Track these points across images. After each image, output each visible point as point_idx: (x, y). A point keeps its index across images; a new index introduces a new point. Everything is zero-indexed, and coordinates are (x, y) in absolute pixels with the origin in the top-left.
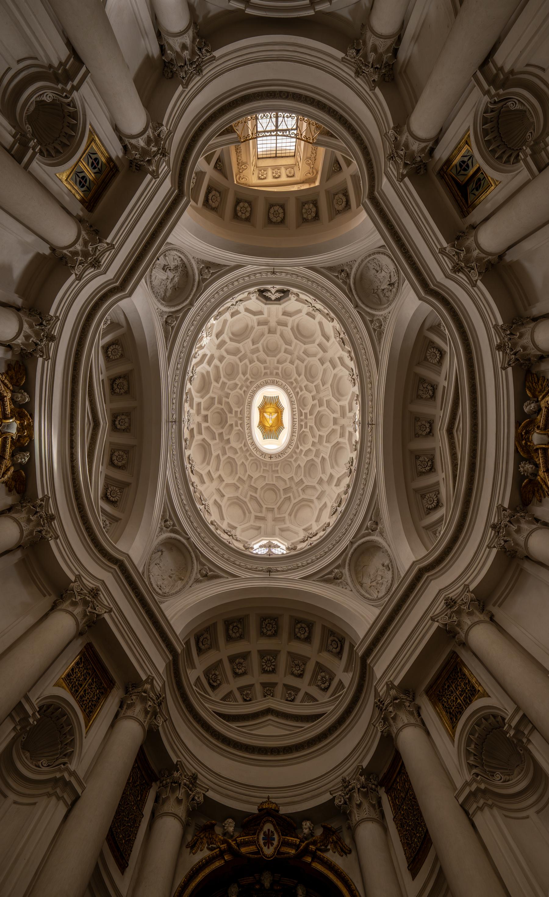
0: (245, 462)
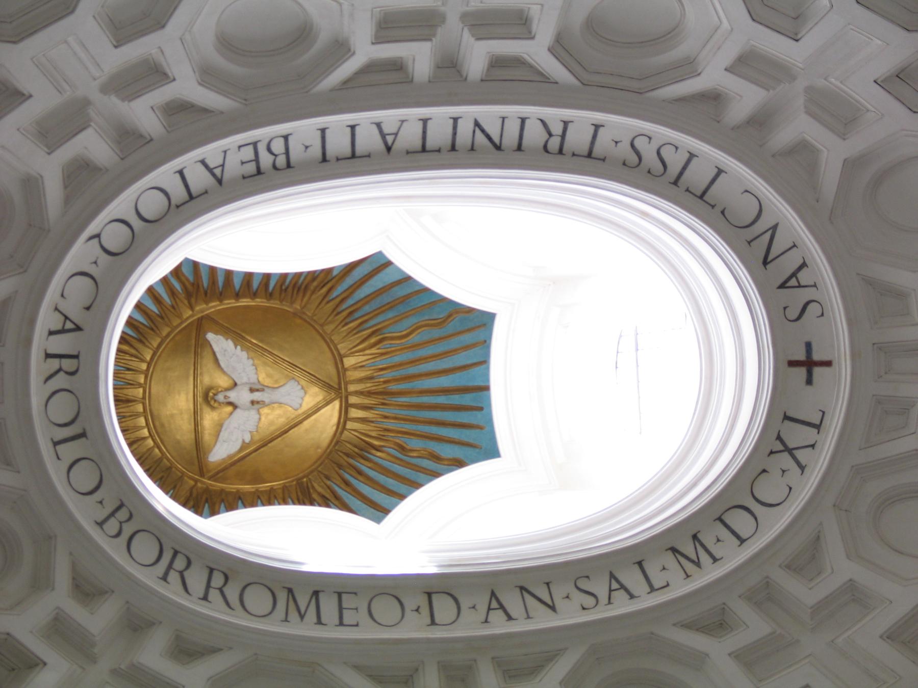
0: (885, 619)
